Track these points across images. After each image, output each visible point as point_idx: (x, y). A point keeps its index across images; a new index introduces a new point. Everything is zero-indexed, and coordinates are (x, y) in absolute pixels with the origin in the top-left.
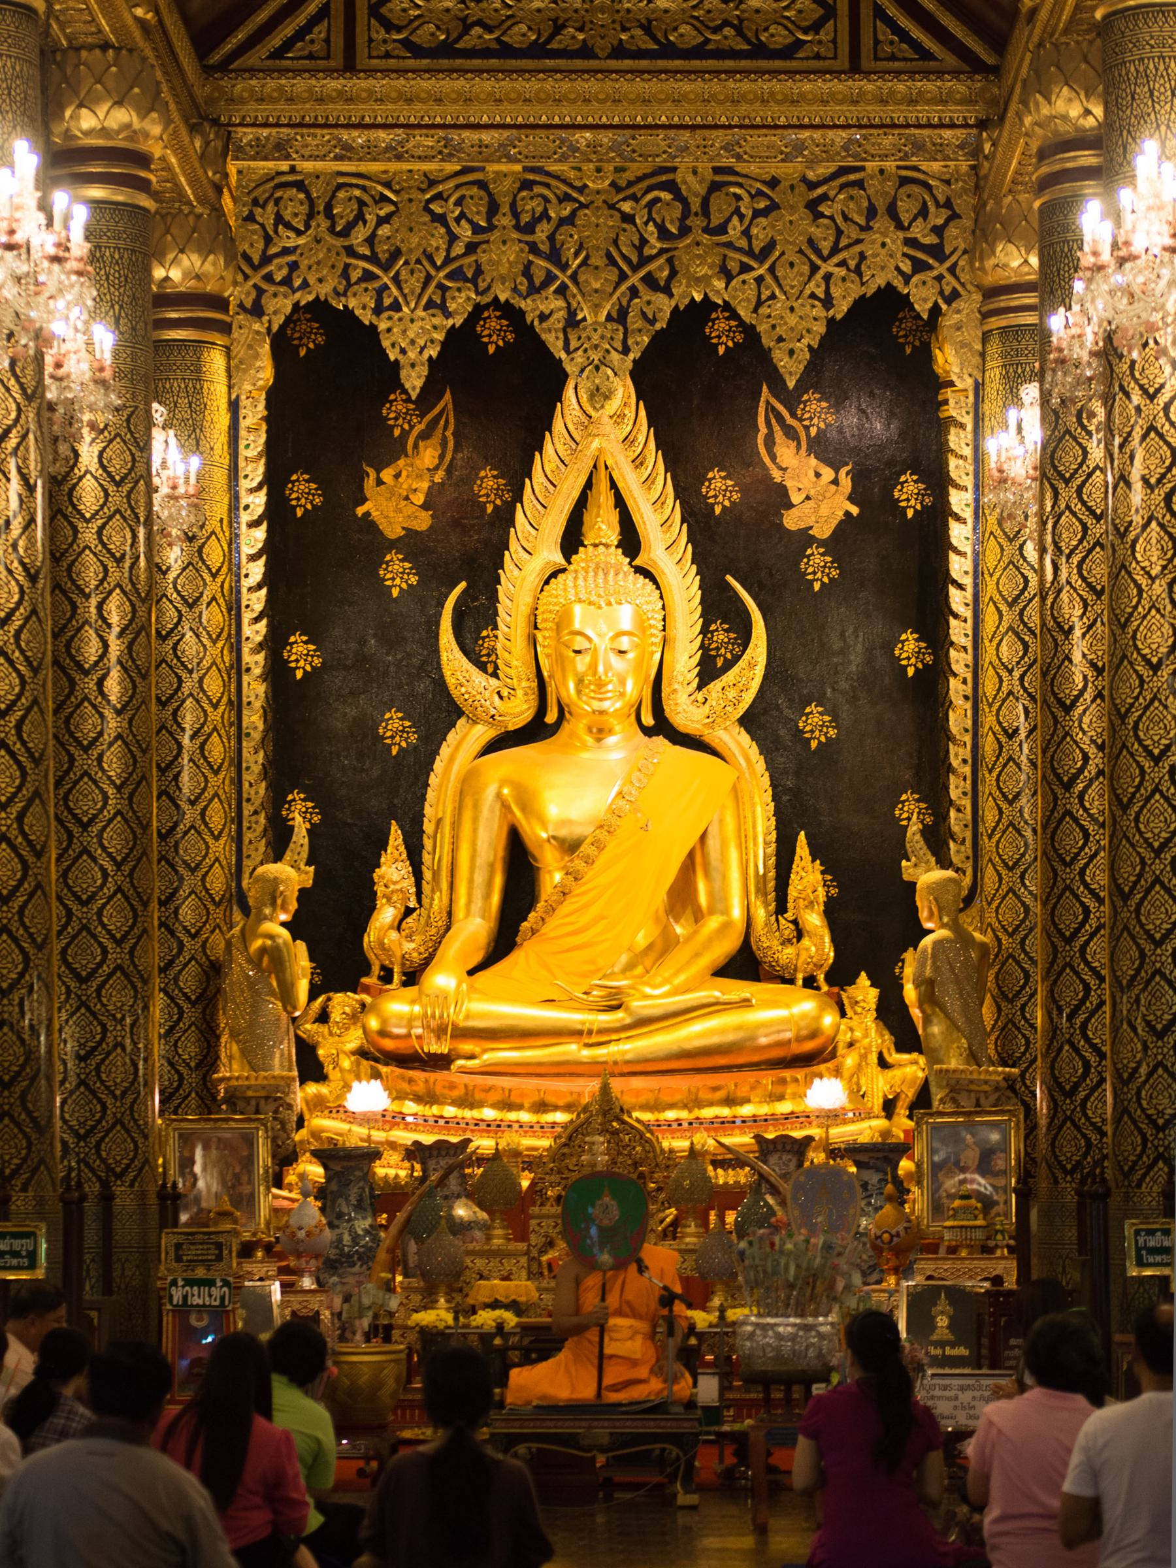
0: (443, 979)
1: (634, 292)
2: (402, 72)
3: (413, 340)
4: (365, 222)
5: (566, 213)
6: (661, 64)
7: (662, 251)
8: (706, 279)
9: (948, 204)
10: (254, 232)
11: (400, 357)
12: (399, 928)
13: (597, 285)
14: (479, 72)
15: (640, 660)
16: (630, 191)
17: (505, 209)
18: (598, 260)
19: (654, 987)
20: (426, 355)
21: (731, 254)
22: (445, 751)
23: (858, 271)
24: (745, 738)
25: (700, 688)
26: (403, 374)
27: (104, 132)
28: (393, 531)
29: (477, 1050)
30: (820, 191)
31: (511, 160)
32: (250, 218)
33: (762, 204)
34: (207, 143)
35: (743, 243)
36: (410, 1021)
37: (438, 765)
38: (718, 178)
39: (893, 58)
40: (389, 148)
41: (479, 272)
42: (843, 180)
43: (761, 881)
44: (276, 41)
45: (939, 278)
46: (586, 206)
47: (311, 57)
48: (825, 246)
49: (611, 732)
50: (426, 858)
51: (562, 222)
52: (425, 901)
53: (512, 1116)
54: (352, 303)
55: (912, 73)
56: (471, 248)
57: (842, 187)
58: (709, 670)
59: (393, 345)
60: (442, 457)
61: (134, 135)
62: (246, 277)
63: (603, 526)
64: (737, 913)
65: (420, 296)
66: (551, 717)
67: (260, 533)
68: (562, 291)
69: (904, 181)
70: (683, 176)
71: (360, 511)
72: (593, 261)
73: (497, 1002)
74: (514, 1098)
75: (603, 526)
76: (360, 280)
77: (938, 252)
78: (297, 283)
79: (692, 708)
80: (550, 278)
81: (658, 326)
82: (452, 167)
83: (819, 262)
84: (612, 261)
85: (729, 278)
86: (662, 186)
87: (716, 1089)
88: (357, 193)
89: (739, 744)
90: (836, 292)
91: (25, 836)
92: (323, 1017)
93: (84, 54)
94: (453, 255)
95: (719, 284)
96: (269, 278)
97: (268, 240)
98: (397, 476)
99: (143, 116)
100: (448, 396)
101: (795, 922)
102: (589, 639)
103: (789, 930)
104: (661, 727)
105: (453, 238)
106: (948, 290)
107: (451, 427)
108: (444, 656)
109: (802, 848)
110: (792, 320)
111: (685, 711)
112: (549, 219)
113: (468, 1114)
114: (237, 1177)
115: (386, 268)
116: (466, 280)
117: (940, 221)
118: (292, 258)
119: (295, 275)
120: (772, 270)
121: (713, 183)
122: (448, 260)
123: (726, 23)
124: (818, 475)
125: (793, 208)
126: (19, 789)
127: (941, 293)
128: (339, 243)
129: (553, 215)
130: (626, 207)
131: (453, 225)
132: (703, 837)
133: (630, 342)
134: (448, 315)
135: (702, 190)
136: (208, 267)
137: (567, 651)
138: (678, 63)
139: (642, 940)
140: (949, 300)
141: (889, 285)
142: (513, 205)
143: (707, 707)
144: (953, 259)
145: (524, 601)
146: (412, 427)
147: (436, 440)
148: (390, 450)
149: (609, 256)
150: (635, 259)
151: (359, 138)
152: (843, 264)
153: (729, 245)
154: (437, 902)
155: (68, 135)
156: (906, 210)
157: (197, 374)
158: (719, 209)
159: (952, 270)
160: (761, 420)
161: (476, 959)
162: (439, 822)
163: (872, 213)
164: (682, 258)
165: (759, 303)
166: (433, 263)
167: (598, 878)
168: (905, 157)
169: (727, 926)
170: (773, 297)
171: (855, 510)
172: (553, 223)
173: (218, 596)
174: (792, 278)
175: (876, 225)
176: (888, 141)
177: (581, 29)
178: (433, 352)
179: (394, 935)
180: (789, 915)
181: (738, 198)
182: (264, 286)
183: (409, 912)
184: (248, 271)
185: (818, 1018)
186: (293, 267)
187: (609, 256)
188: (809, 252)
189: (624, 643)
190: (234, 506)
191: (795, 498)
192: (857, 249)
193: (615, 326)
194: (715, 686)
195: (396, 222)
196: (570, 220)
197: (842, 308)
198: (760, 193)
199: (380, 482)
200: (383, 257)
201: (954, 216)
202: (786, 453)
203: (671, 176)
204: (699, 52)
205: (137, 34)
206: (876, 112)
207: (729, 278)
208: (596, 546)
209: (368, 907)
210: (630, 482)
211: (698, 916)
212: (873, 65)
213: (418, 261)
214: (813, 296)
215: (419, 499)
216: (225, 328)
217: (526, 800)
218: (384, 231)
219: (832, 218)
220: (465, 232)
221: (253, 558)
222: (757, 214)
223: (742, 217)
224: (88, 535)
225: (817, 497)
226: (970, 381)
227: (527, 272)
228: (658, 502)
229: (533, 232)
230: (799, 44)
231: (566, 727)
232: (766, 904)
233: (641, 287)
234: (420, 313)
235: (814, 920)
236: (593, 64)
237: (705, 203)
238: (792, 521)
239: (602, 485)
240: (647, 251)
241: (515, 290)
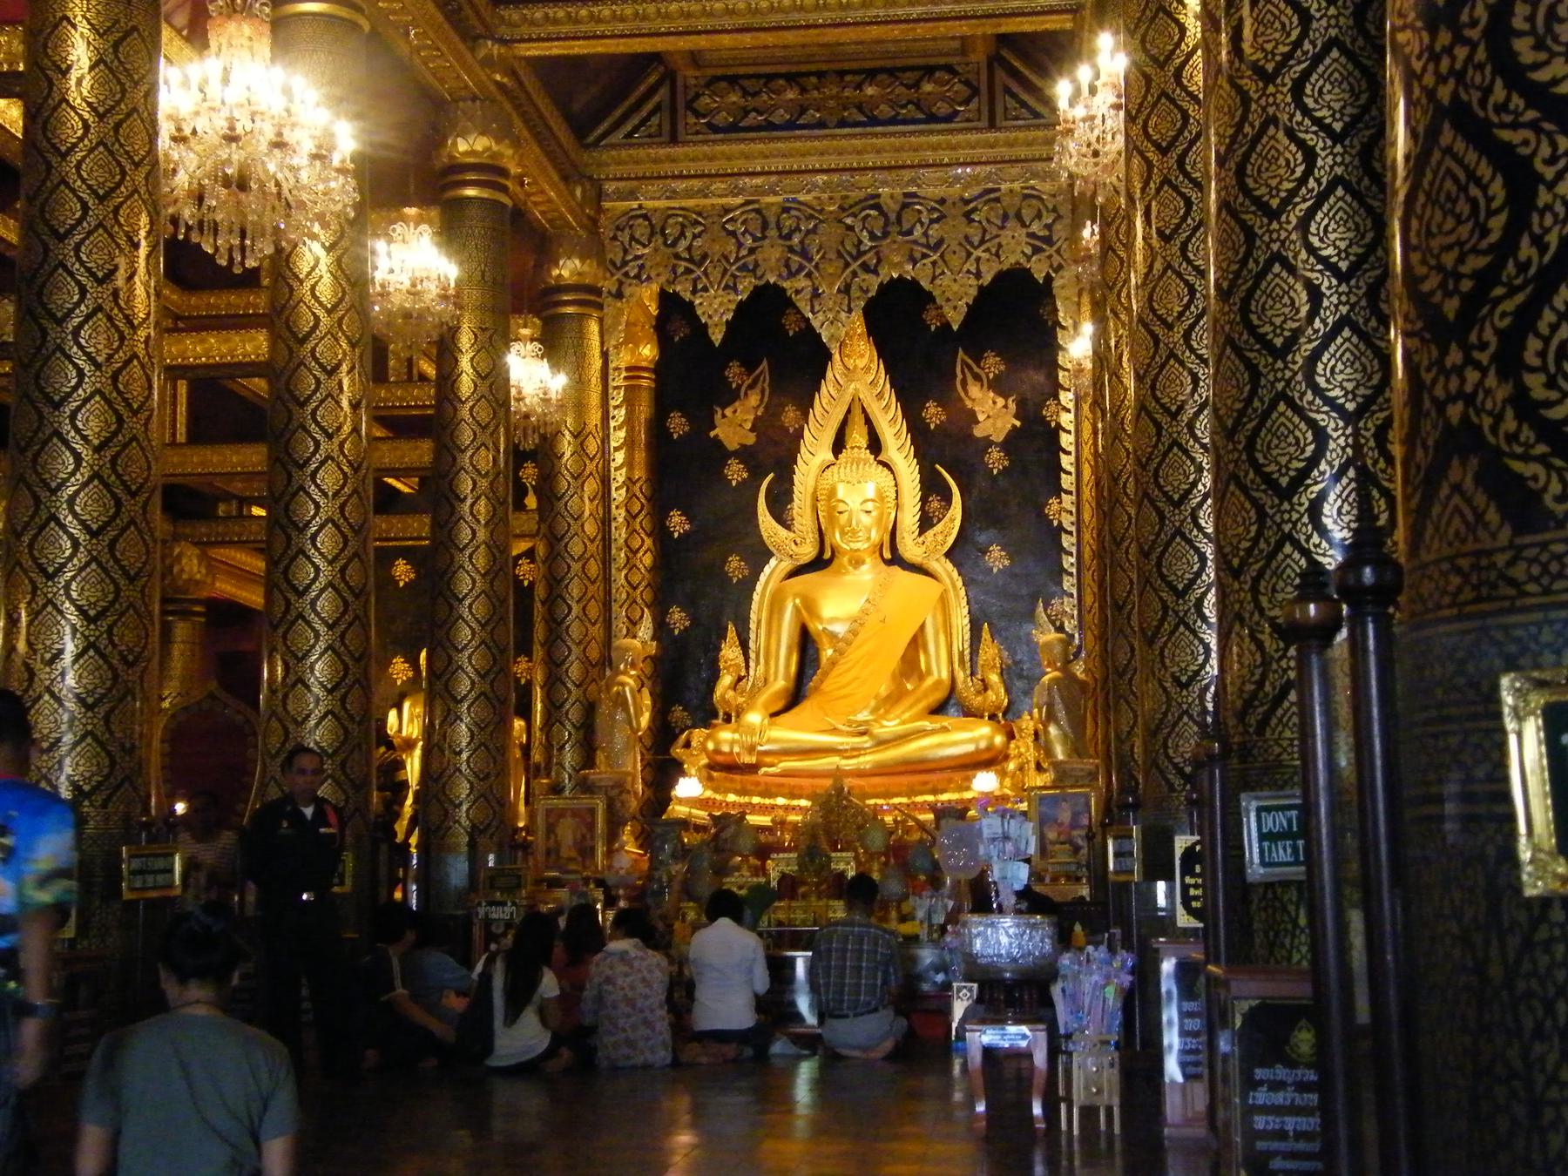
0: (754, 718)
1: (855, 274)
2: (705, 142)
3: (715, 310)
6: (869, 129)
7: (872, 248)
8: (900, 264)
9: (1055, 210)
12: (735, 689)
13: (831, 271)
14: (753, 140)
15: (881, 515)
17: (773, 225)
18: (833, 255)
22: (763, 578)
23: (997, 255)
24: (949, 566)
25: (920, 534)
26: (710, 331)
27: (472, 153)
28: (732, 444)
31: (776, 194)
32: (615, 238)
34: (584, 192)
35: (923, 240)
36: (732, 743)
37: (759, 587)
39: (1017, 118)
40: (700, 191)
41: (757, 265)
43: (961, 654)
44: (628, 127)
45: (1050, 257)
47: (650, 136)
48: (976, 240)
49: (863, 562)
50: (752, 645)
51: (808, 232)
52: (752, 672)
53: (795, 802)
54: (678, 288)
55: (1028, 127)
56: (752, 251)
57: (986, 203)
58: (926, 523)
61: (494, 156)
63: (858, 437)
64: (945, 675)
66: (827, 555)
67: (622, 434)
68: (809, 275)
69: (1026, 197)
70: (885, 201)
71: (712, 434)
73: (788, 732)
74: (796, 792)
75: (858, 437)
77: (1048, 240)
80: (801, 268)
82: (739, 200)
86: (872, 207)
87: (925, 783)
89: (945, 568)
90: (983, 268)
91: (347, 583)
92: (687, 745)
93: (461, 104)
96: (626, 274)
97: (626, 252)
99: (497, 143)
100: (765, 363)
103: (979, 685)
104: (897, 560)
105: (740, 245)
108: (761, 519)
109: (986, 634)
110: (955, 287)
111: (911, 548)
113: (767, 801)
114: (584, 837)
122: (737, 259)
123: (910, 102)
125: (954, 218)
126: (342, 550)
128: (670, 250)
130: (849, 221)
132: (922, 627)
135: (897, 207)
136: (586, 268)
137: (833, 514)
138: (879, 129)
139: (883, 690)
140: (1056, 271)
141: (1018, 263)
145: (811, 483)
147: (758, 390)
149: (839, 252)
150: (854, 252)
151: (681, 185)
153: (915, 242)
154: (756, 671)
155: (452, 157)
156: (1027, 214)
157: (582, 335)
158: (908, 219)
159: (1058, 251)
161: (780, 705)
162: (759, 622)
163: (1005, 217)
164: (885, 251)
165: (934, 278)
167: (854, 654)
168: (1027, 180)
169: (939, 682)
170: (943, 273)
171: (1018, 423)
174: (955, 261)
175: (1008, 225)
176: (1016, 170)
177: (818, 110)
178: (730, 316)
179: (731, 693)
181: (920, 212)
183: (740, 679)
185: (991, 738)
187: (839, 252)
189: (869, 506)
190: (606, 418)
191: (981, 417)
194: (930, 533)
196: (814, 231)
197: (987, 279)
198: (934, 209)
199: (724, 416)
200: (697, 258)
201: (1059, 217)
202: (975, 390)
204: (893, 121)
205: (493, 88)
206: (1006, 152)
207: (914, 262)
209: (715, 676)
210: (875, 409)
211: (922, 677)
212: (1005, 123)
214: (968, 272)
215: (748, 426)
216: (600, 307)
217: (809, 605)
218: (698, 243)
220: (749, 242)
224: (465, 412)
225: (992, 415)
227: (787, 266)
228: (893, 420)
230: (956, 113)
231: (836, 562)
232: (964, 669)
233: (859, 272)
234: (720, 292)
235: (994, 678)
236: (827, 131)
238: (978, 432)
239: (857, 411)
240: (863, 248)
241: (780, 276)
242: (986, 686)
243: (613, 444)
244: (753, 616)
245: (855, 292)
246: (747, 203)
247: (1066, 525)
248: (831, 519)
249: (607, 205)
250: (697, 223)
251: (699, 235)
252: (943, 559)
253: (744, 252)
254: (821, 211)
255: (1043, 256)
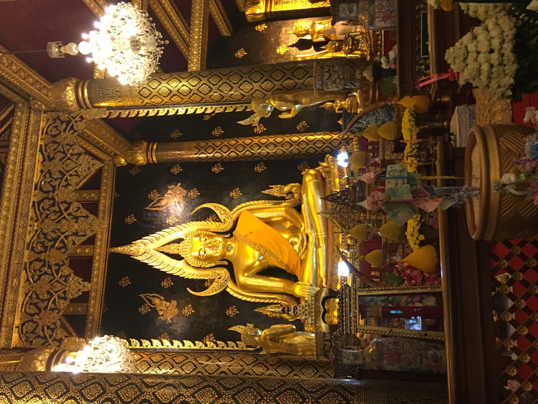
4: (37, 303)
5: (43, 236)
7: (59, 206)
9: (54, 120)
10: (36, 341)
11: (81, 291)
16: (39, 216)
19: (301, 226)
20: (81, 282)
21: (61, 184)
24: (235, 209)
29: (320, 279)
30: (46, 158)
33: (48, 175)
35: (59, 180)
38: (38, 188)
42: (43, 150)
43: (275, 204)
45: (76, 122)
46: (42, 229)
48: (62, 155)
50: (267, 301)
51: (45, 238)
52: (280, 302)
56: (50, 267)
59: (77, 293)
60: (157, 297)
62: (50, 344)
64: (283, 209)
65: (63, 284)
66: (226, 263)
68: (66, 237)
69: (47, 133)
72: (59, 227)
76: (55, 305)
77: (68, 123)
78: (53, 326)
79: (227, 224)
80: (62, 241)
81: (81, 206)
82: (23, 273)
83: (67, 157)
84: (59, 221)
85: (69, 184)
86: (39, 206)
88: (28, 305)
90: (76, 151)
94: (51, 273)
95: (70, 188)
97: (39, 336)
98: (161, 310)
100: (141, 295)
101: (287, 194)
102: (201, 249)
106: (80, 119)
107: (149, 294)
108: (208, 295)
109: (266, 192)
111: (228, 226)
112: (44, 241)
115: (52, 295)
116: (59, 269)
117: (59, 122)
118: (45, 328)
119: (51, 327)
120: (68, 171)
121: (40, 190)
124: (170, 194)
127: (80, 121)
128: (43, 312)
129: (43, 240)
131: (42, 273)
132: (260, 219)
133: (84, 215)
134: (70, 275)
142: (38, 253)
143: (227, 219)
144: (71, 118)
146: (148, 306)
148: (154, 311)
150: (60, 214)
152: (68, 150)
153: (59, 185)
159: (74, 118)
160: (154, 209)
163: (55, 142)
165: (77, 175)
166: (53, 279)
170: (76, 171)
171: (179, 184)
172: (46, 240)
173: (150, 356)
178: (80, 280)
180: (285, 196)
181: (45, 182)
182: (53, 338)
184: (48, 344)
186: (48, 327)
187: (57, 222)
188: (63, 161)
189: (203, 239)
192: (65, 146)
193: (79, 220)
195: (38, 293)
198: (44, 176)
199: (163, 315)
200: (49, 296)
201: (58, 118)
203: (36, 203)
207: (69, 184)
208: (179, 250)
213: (52, 285)
214: (77, 159)
215: (168, 304)
217: (248, 269)
219: (55, 154)
220: (46, 269)
221: (141, 345)
222: (51, 177)
223: (51, 181)
226: (107, 112)
229: (47, 247)
232: (282, 203)
233: (68, 212)
234: (68, 284)
235: (286, 189)
237: (45, 192)
242: (290, 193)
243: (138, 346)
244: (253, 300)
245: (78, 214)
246: (25, 269)
247: (202, 111)
248: (209, 258)
249: (13, 345)
250: (31, 297)
251: (37, 295)
252: (232, 212)
253: (49, 271)
254: (36, 231)
255: (75, 125)
